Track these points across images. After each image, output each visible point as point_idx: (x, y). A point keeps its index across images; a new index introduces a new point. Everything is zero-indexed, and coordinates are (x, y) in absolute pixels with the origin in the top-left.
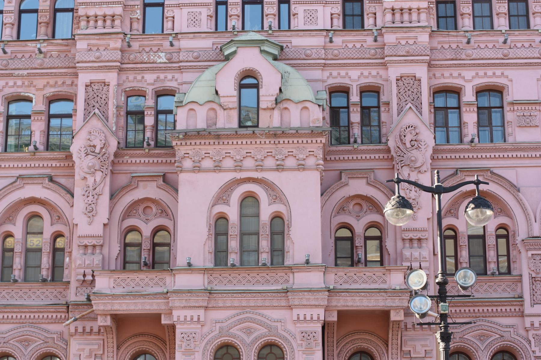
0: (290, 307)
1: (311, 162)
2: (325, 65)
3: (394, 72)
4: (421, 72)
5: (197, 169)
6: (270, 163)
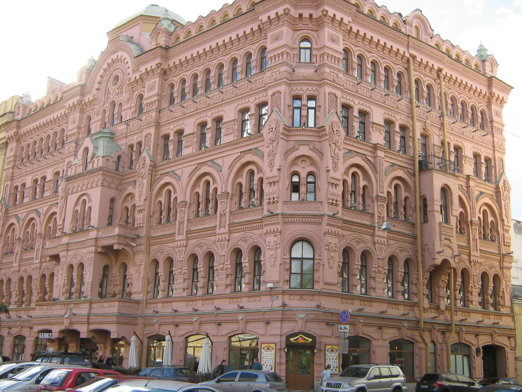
4: (152, 130)
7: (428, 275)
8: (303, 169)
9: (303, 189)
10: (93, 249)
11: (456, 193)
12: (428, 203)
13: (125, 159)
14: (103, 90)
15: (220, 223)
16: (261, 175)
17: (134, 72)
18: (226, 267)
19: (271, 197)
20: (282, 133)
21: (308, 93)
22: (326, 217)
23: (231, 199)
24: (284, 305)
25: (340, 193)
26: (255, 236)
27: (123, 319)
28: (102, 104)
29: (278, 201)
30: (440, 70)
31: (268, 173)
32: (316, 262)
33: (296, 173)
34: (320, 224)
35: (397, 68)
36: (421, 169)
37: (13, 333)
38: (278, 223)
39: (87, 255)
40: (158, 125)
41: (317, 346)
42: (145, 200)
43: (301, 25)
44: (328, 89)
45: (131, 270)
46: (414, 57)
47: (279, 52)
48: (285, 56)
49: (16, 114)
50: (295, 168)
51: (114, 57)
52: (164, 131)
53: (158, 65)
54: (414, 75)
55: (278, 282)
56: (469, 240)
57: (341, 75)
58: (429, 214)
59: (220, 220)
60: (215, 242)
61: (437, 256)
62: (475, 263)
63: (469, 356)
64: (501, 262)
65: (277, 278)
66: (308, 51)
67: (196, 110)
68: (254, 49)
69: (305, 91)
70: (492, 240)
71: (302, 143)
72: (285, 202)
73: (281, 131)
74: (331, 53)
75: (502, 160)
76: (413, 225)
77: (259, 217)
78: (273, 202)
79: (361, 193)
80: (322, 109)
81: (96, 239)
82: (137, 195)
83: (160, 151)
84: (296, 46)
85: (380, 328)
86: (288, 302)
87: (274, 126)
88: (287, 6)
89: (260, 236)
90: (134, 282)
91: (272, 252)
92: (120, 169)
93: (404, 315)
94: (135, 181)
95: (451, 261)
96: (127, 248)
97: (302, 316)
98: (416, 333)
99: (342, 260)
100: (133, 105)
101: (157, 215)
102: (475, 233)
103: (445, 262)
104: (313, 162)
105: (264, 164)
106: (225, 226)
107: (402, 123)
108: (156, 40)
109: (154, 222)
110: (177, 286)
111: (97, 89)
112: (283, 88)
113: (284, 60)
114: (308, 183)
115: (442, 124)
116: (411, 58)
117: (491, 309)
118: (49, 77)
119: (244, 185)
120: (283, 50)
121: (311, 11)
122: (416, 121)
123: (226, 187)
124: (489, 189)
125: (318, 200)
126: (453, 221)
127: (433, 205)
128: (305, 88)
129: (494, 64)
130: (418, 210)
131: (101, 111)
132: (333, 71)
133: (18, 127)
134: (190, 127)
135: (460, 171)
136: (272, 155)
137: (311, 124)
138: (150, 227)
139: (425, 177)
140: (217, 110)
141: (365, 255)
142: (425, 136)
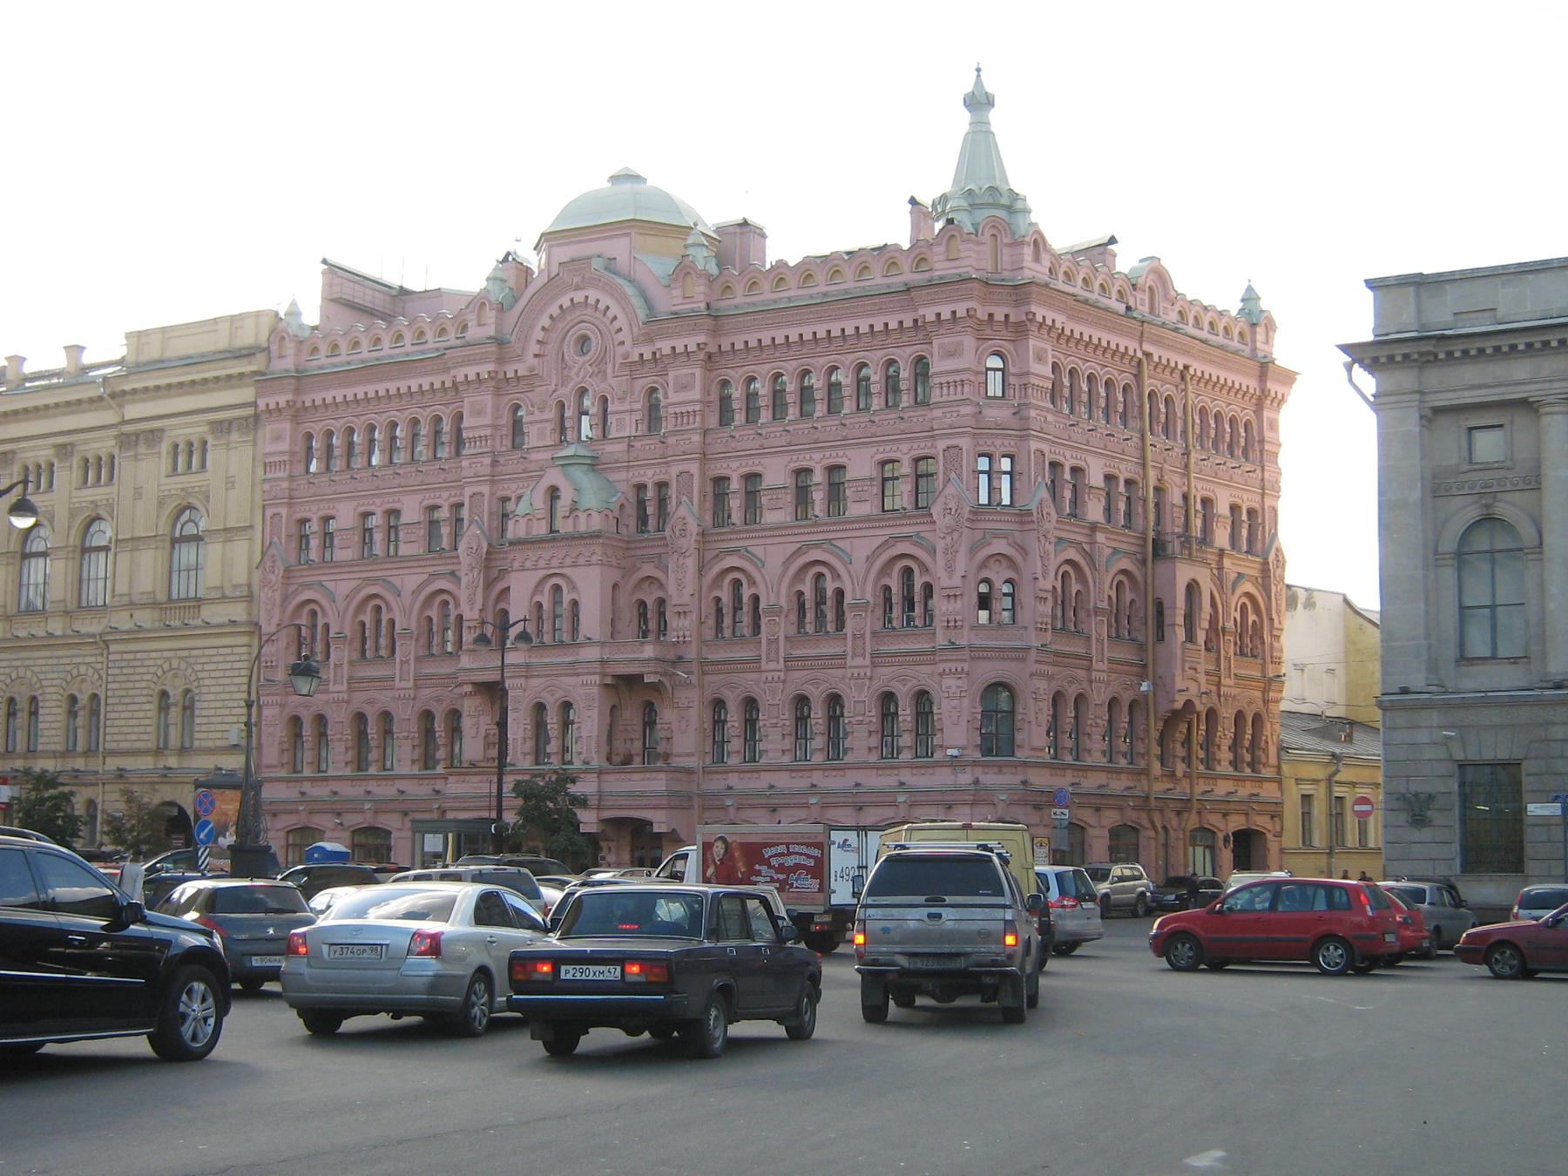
0: (578, 675)
1: (595, 559)
4: (694, 468)
6: (568, 561)
7: (1161, 724)
8: (998, 574)
9: (996, 606)
11: (1207, 586)
12: (1167, 612)
13: (631, 510)
16: (926, 579)
17: (635, 342)
22: (1034, 651)
24: (977, 782)
26: (923, 675)
27: (678, 801)
28: (553, 387)
30: (1186, 367)
31: (943, 580)
33: (986, 580)
34: (1024, 660)
36: (1155, 554)
37: (347, 824)
40: (704, 458)
45: (666, 715)
46: (1148, 355)
47: (958, 378)
48: (967, 388)
49: (274, 354)
50: (985, 574)
51: (579, 297)
52: (719, 469)
54: (1149, 384)
55: (963, 748)
56: (1218, 659)
57: (1050, 418)
58: (1166, 629)
61: (1177, 697)
62: (1226, 697)
63: (1211, 848)
64: (1265, 691)
65: (963, 741)
68: (905, 357)
70: (1254, 656)
71: (998, 535)
75: (1275, 510)
76: (1142, 647)
77: (927, 646)
80: (1024, 477)
83: (709, 505)
85: (1098, 809)
86: (982, 778)
88: (971, 304)
89: (931, 675)
93: (1129, 788)
95: (1197, 703)
98: (1143, 815)
100: (638, 406)
101: (711, 622)
102: (1228, 647)
103: (1189, 703)
105: (939, 568)
106: (863, 655)
107: (1129, 476)
109: (709, 634)
110: (769, 747)
111: (536, 356)
115: (1187, 466)
117: (1248, 771)
118: (333, 271)
120: (964, 377)
121: (1006, 310)
123: (863, 590)
124: (1251, 567)
126: (1201, 637)
127: (1174, 615)
129: (1270, 326)
132: (1041, 412)
135: (1211, 544)
136: (951, 552)
138: (703, 642)
139: (1162, 568)
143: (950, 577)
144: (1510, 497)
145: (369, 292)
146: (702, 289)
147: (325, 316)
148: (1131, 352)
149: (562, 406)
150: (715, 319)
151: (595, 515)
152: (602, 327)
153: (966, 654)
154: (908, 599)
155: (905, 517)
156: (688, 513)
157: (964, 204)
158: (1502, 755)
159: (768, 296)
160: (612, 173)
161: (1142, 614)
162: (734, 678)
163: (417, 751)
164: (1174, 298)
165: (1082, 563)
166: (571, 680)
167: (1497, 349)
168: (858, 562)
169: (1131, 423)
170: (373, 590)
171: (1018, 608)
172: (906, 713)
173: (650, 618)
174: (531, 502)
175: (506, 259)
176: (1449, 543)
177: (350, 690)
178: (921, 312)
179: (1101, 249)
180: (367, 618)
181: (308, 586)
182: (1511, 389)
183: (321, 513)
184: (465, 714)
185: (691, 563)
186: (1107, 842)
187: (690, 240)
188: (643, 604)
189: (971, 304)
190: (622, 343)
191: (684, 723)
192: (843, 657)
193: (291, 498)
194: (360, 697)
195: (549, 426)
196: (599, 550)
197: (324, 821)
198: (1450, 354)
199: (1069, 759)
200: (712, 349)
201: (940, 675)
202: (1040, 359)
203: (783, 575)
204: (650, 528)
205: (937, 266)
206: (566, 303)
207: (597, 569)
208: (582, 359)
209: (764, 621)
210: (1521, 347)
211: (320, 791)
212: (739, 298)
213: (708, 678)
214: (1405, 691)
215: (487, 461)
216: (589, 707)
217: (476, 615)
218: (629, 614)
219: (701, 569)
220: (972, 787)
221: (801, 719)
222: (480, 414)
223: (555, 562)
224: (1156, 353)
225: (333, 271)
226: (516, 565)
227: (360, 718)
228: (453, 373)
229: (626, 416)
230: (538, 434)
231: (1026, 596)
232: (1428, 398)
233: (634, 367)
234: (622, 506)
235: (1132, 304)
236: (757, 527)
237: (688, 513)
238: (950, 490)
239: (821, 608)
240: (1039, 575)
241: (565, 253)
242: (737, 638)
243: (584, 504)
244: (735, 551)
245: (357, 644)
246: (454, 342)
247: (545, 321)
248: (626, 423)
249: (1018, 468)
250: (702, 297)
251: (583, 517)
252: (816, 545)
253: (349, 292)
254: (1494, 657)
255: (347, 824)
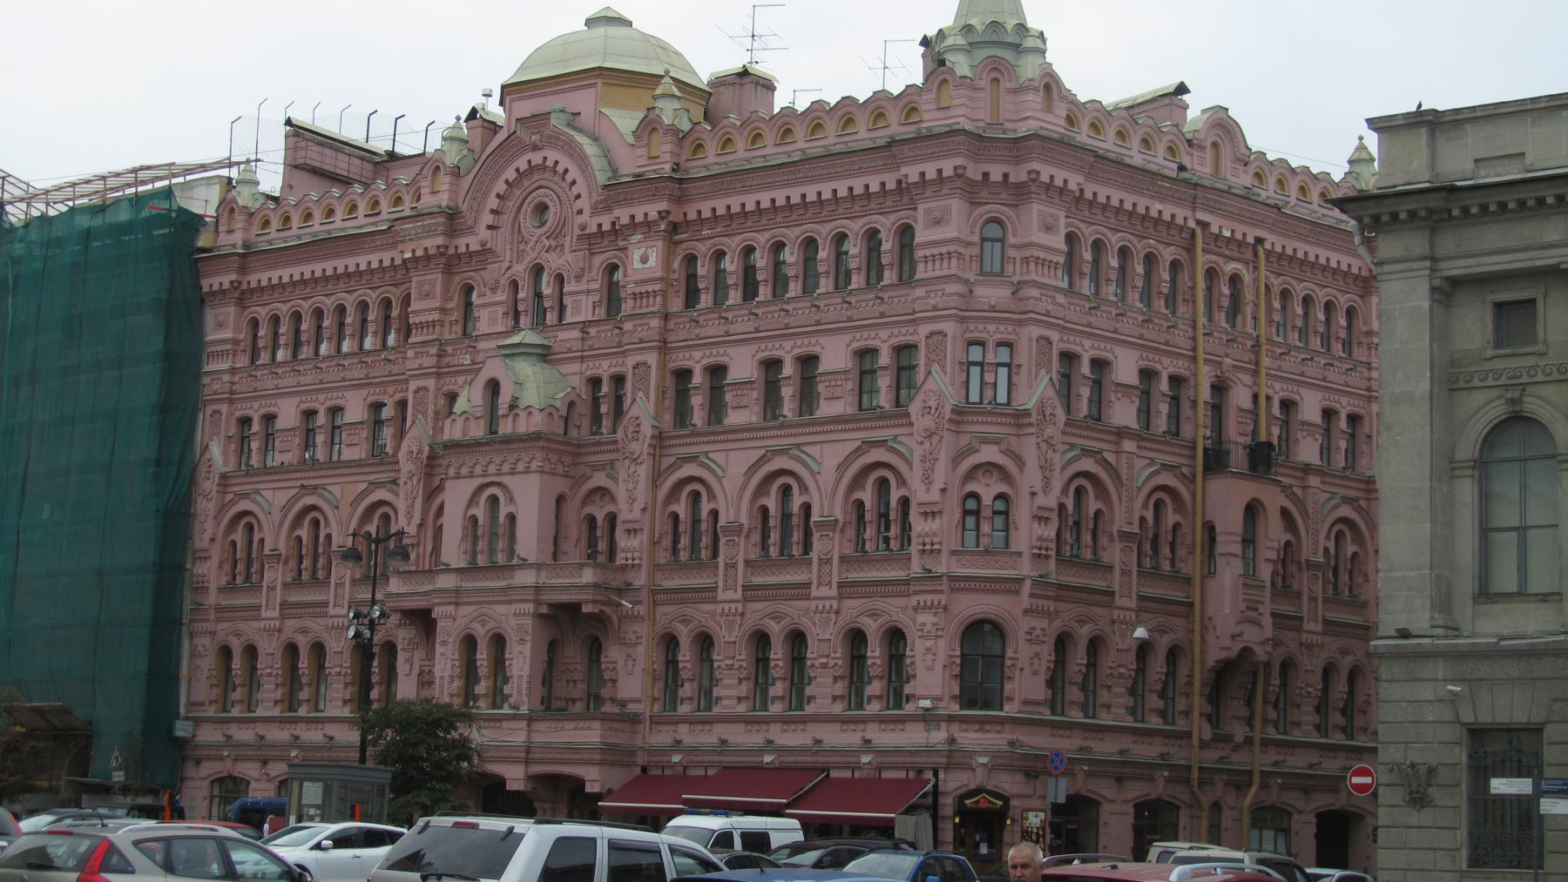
0: (511, 602)
1: (535, 465)
2: (582, 357)
3: (631, 361)
4: (652, 359)
5: (458, 477)
6: (506, 468)
8: (987, 490)
10: (530, 607)
13: (583, 409)
14: (506, 230)
15: (819, 576)
16: (903, 492)
17: (596, 210)
18: (832, 663)
19: (928, 540)
20: (950, 420)
21: (998, 336)
22: (1028, 583)
23: (842, 531)
24: (952, 741)
25: (1053, 535)
26: (896, 610)
28: (506, 264)
29: (939, 551)
30: (1259, 241)
31: (920, 494)
32: (1008, 663)
33: (974, 495)
34: (1017, 593)
35: (1168, 254)
38: (941, 592)
39: (517, 622)
40: (664, 347)
41: (1011, 813)
42: (644, 510)
43: (984, 194)
44: (1036, 331)
45: (613, 653)
46: (1204, 225)
47: (944, 250)
48: (954, 262)
50: (972, 487)
51: (536, 158)
52: (679, 361)
53: (663, 215)
54: (1202, 261)
55: (940, 699)
57: (1060, 298)
59: (819, 570)
60: (807, 611)
65: (938, 692)
66: (998, 245)
67: (757, 331)
68: (886, 225)
69: (993, 332)
72: (953, 553)
73: (948, 416)
74: (1042, 255)
78: (930, 552)
79: (1091, 526)
80: (1024, 371)
81: (538, 589)
82: (621, 493)
83: (669, 402)
84: (976, 239)
86: (957, 735)
87: (933, 404)
88: (959, 161)
89: (904, 609)
90: (622, 678)
91: (929, 644)
92: (573, 433)
94: (612, 462)
96: (608, 610)
97: (984, 760)
99: (1053, 658)
100: (596, 286)
103: (1246, 651)
104: (1005, 475)
105: (914, 477)
106: (830, 583)
108: (648, 145)
109: (663, 557)
110: (724, 693)
111: (489, 227)
112: (949, 327)
113: (953, 271)
114: (995, 513)
116: (1199, 231)
118: (297, 133)
119: (868, 505)
120: (952, 248)
122: (1201, 362)
123: (832, 506)
125: (1013, 549)
128: (991, 328)
130: (1198, 548)
131: (504, 281)
133: (243, 270)
134: (743, 365)
136: (930, 459)
137: (1002, 397)
138: (657, 567)
140: (806, 341)
141: (1095, 645)
142: (1220, 388)
143: (928, 490)
144: (1544, 391)
145: (358, 162)
146: (667, 148)
147: (287, 186)
148: (1180, 221)
149: (514, 285)
150: (679, 185)
151: (536, 413)
152: (563, 196)
153: (945, 585)
154: (882, 516)
155: (881, 417)
156: (644, 409)
157: (961, 41)
158: (1520, 717)
159: (741, 154)
160: (589, 14)
161: (1188, 541)
162: (688, 610)
163: (350, 689)
164: (1245, 158)
165: (1103, 475)
166: (502, 609)
167: (1522, 204)
168: (825, 469)
169: (1182, 309)
170: (310, 500)
171: (1012, 527)
172: (875, 653)
173: (600, 538)
174: (470, 398)
175: (473, 114)
176: (1467, 449)
177: (283, 617)
178: (904, 170)
179: (1166, 101)
180: (304, 533)
181: (245, 496)
182: (1540, 253)
183: (263, 411)
184: (399, 647)
185: (643, 471)
186: (1130, 819)
187: (659, 91)
188: (592, 520)
189: (959, 161)
190: (580, 212)
191: (630, 663)
192: (807, 585)
193: (233, 393)
194: (291, 624)
195: (501, 310)
196: (539, 455)
197: (249, 770)
198: (1465, 211)
199: (1076, 716)
200: (676, 217)
201: (915, 609)
202: (1048, 228)
203: (744, 488)
204: (604, 430)
205: (926, 116)
206: (523, 166)
207: (537, 476)
208: (539, 232)
209: (723, 540)
210: (1550, 200)
211: (244, 734)
212: (711, 160)
213: (661, 610)
214: (1404, 634)
215: (433, 350)
216: (522, 641)
217: (412, 530)
218: (574, 530)
219: (656, 479)
220: (946, 747)
221: (762, 662)
222: (428, 300)
223: (492, 469)
224: (1215, 224)
225: (297, 133)
226: (452, 472)
227: (292, 650)
228: (400, 247)
229: (583, 297)
230: (489, 320)
231: (1022, 513)
232: (1444, 265)
233: (592, 240)
234: (571, 404)
235: (1186, 162)
236: (718, 428)
237: (644, 409)
238: (930, 385)
239: (786, 529)
240: (1038, 489)
241: (526, 108)
242: (695, 563)
243: (523, 403)
244: (693, 459)
245: (293, 564)
246: (408, 213)
247: (500, 187)
248: (582, 308)
249: (1016, 362)
250: (667, 157)
251: (523, 416)
252: (782, 452)
253: (315, 156)
254: (1521, 595)
255: (273, 773)
